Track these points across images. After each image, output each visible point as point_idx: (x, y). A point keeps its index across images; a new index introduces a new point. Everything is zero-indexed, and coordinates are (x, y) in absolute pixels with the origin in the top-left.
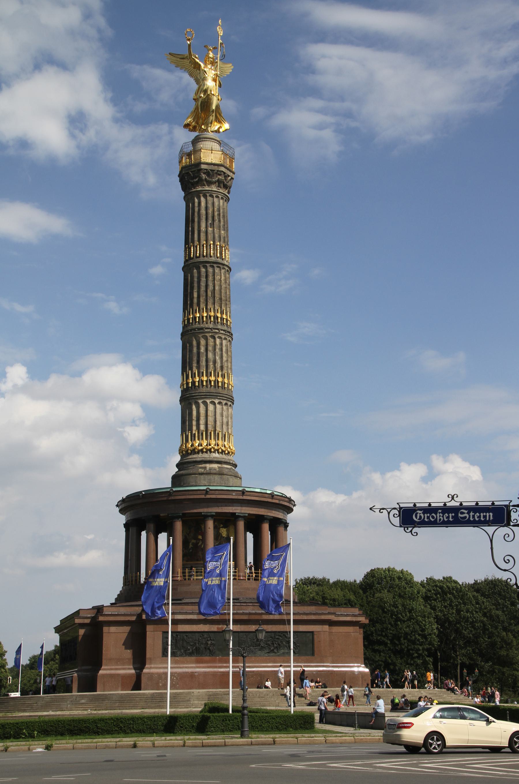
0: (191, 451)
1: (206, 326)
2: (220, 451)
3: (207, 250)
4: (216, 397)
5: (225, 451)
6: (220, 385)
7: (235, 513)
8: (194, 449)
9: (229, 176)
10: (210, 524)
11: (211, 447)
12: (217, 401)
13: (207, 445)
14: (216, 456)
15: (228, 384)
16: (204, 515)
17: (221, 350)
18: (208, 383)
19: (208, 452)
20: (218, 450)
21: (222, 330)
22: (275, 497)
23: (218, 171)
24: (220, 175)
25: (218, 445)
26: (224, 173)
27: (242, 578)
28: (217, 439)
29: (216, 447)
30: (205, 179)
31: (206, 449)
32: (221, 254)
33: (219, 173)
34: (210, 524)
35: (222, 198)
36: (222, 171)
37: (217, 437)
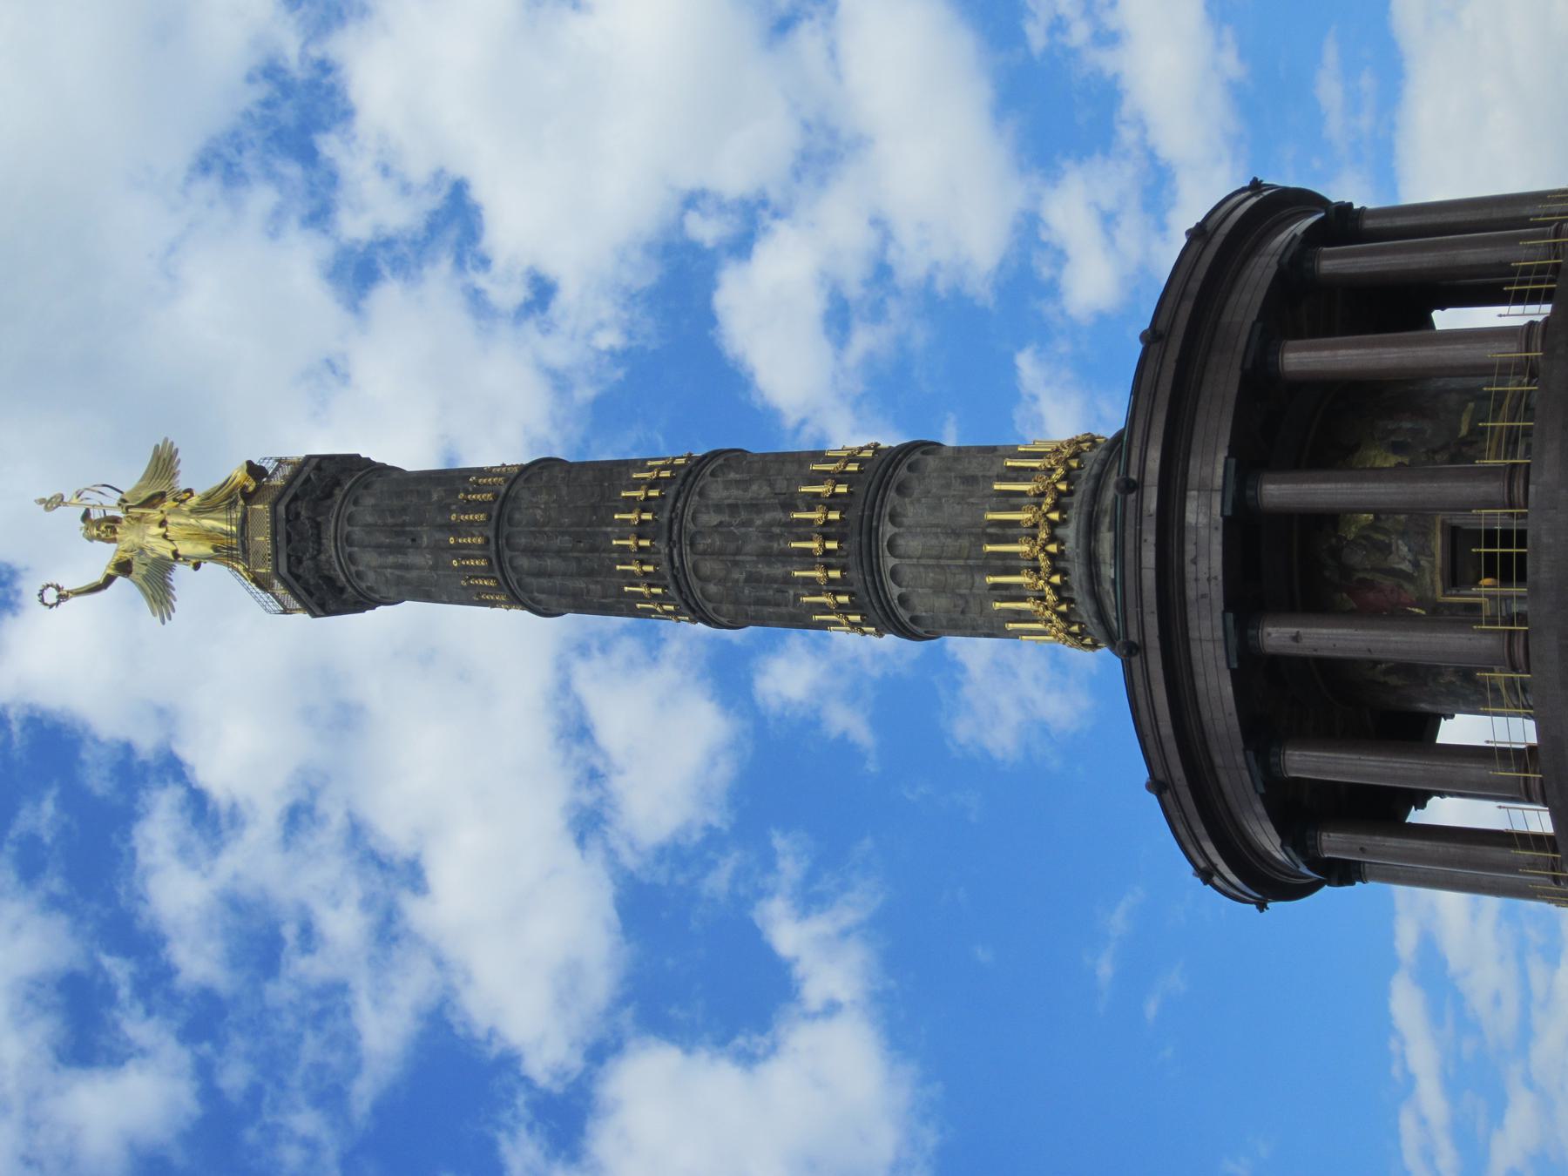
0: (1073, 624)
1: (665, 564)
2: (1055, 516)
3: (475, 558)
4: (873, 533)
5: (1060, 494)
6: (834, 516)
7: (1228, 522)
8: (1062, 616)
9: (308, 479)
10: (1277, 636)
11: (1042, 556)
12: (888, 530)
13: (1037, 570)
14: (1070, 532)
15: (839, 478)
16: (1239, 659)
17: (734, 508)
18: (833, 560)
19: (1062, 564)
20: (1053, 525)
21: (674, 506)
22: (1162, 326)
23: (288, 521)
24: (298, 515)
25: (1036, 526)
26: (295, 498)
27: (1518, 492)
28: (1015, 531)
29: (1043, 535)
30: (314, 558)
31: (1054, 570)
32: (479, 506)
33: (292, 518)
34: (1277, 636)
35: (356, 503)
36: (287, 507)
37: (1010, 532)
